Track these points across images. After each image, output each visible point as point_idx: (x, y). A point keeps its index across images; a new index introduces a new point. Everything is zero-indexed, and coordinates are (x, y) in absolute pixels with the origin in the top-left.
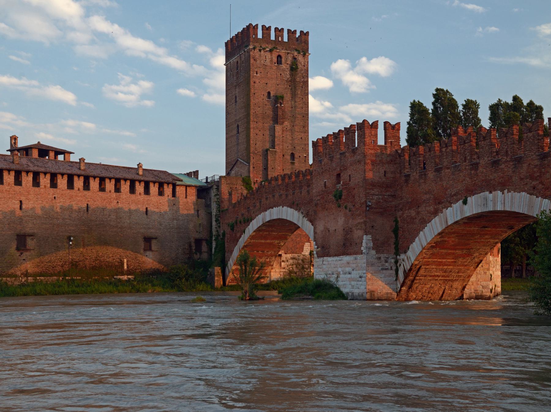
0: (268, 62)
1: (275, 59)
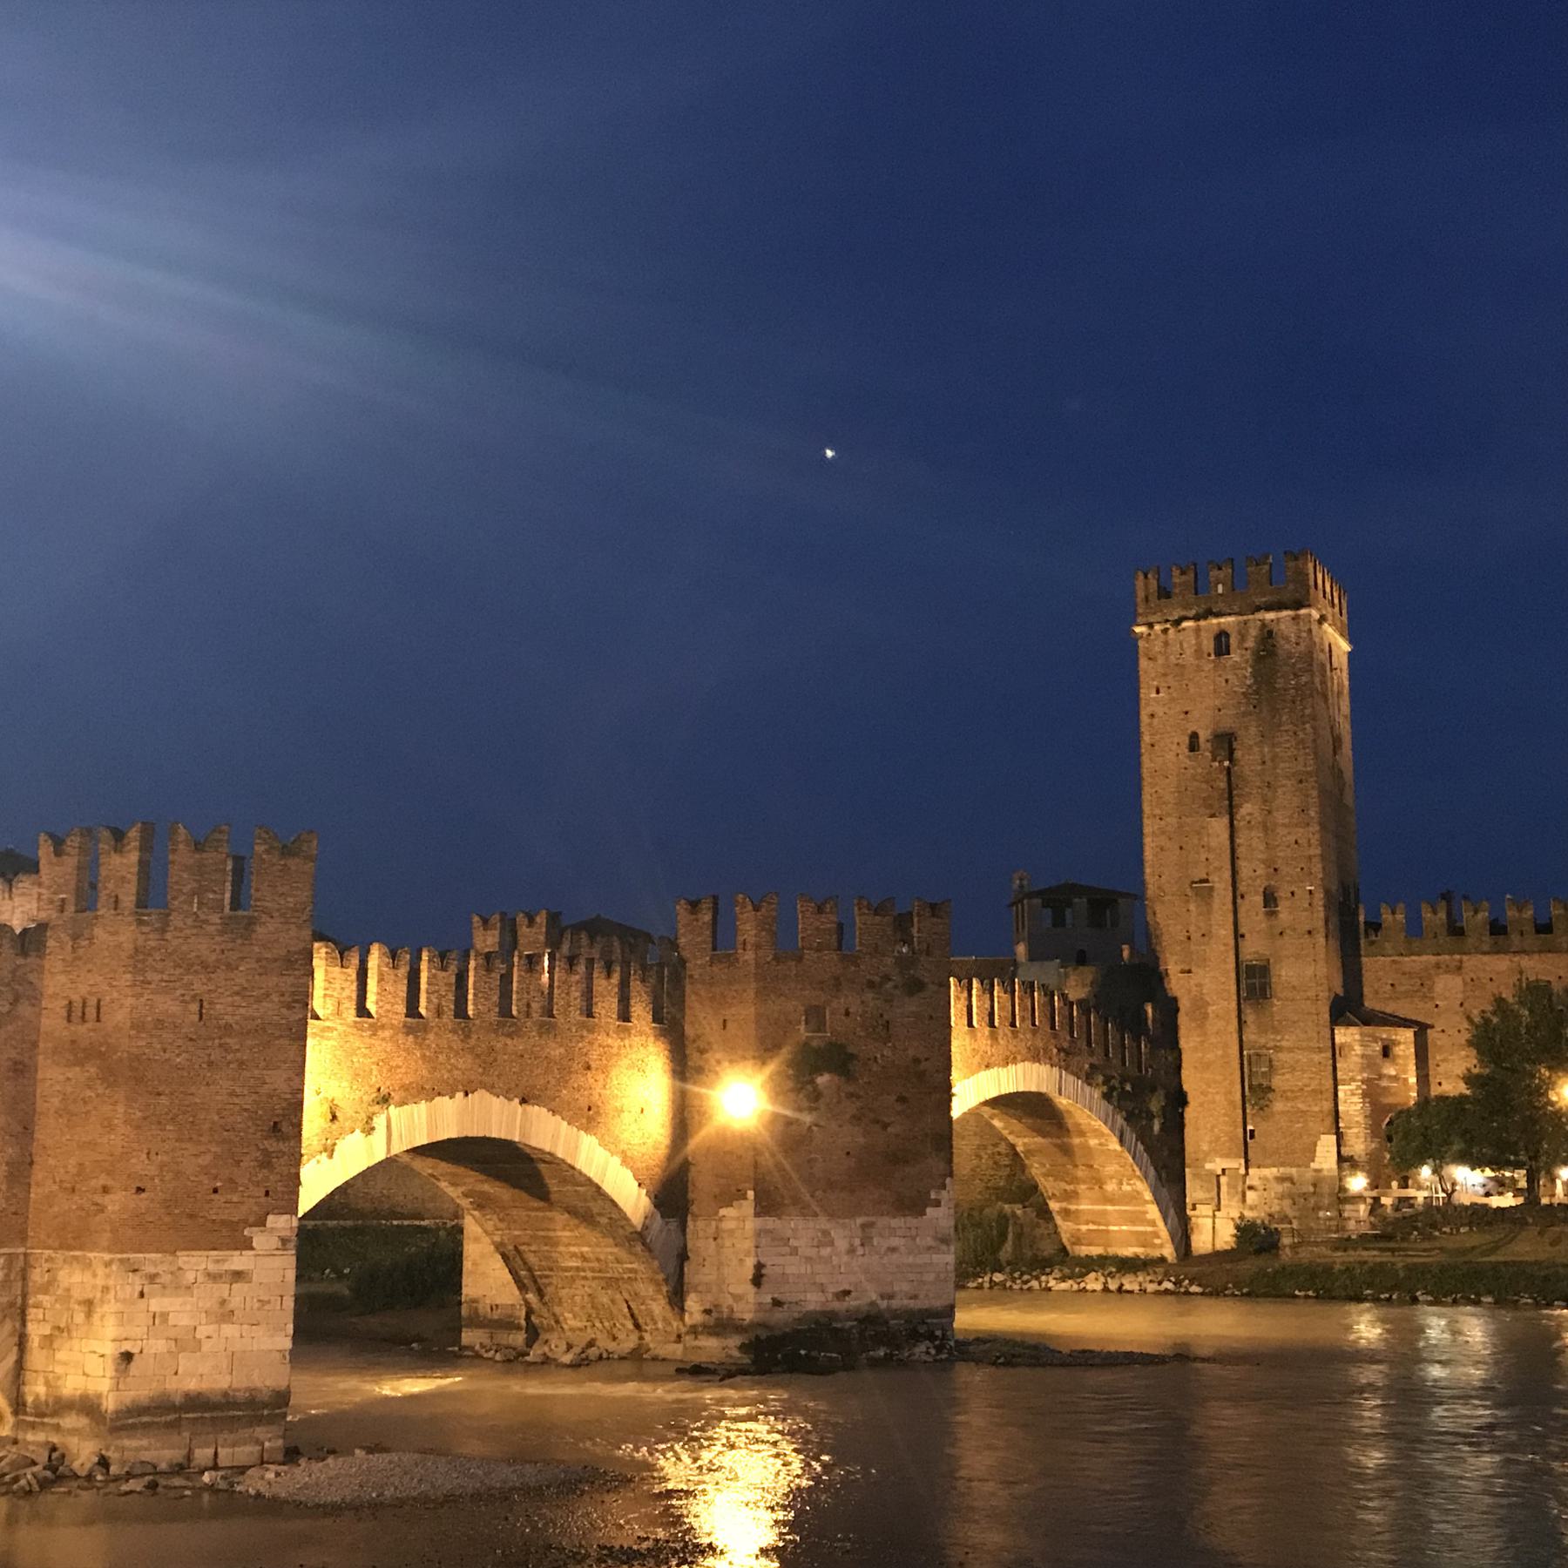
0: (1189, 658)
1: (1208, 645)
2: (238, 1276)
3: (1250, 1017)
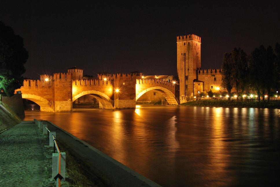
1: (184, 44)
2: (67, 103)
3: (186, 81)
